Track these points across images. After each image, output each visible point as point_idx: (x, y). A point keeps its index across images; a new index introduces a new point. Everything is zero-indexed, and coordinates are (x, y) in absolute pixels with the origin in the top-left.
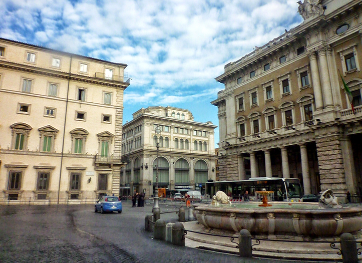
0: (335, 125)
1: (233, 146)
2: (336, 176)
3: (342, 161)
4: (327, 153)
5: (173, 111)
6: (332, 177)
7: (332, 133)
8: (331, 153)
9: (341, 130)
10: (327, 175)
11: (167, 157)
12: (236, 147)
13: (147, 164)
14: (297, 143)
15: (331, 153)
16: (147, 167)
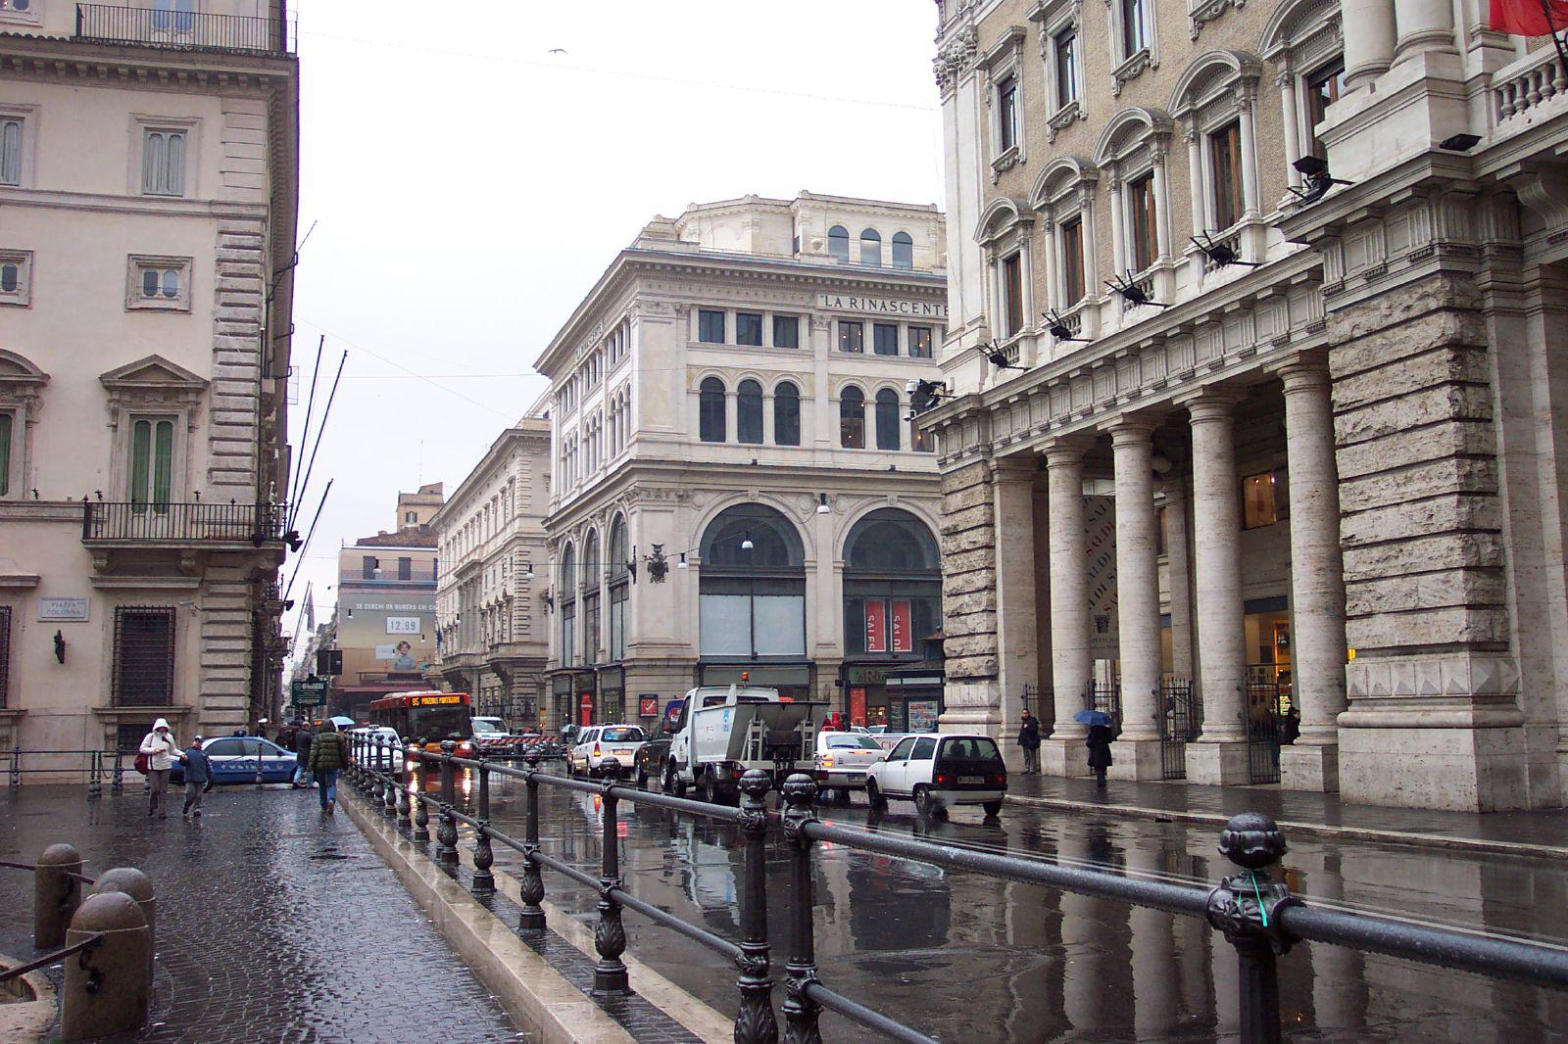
0: (1426, 194)
1: (962, 410)
2: (1428, 590)
3: (1490, 475)
4: (1386, 415)
5: (835, 219)
6: (1410, 605)
7: (1416, 259)
8: (1403, 414)
9: (1489, 233)
10: (1383, 587)
11: (791, 500)
12: (981, 413)
13: (657, 547)
14: (1268, 358)
15: (1403, 414)
16: (658, 570)
